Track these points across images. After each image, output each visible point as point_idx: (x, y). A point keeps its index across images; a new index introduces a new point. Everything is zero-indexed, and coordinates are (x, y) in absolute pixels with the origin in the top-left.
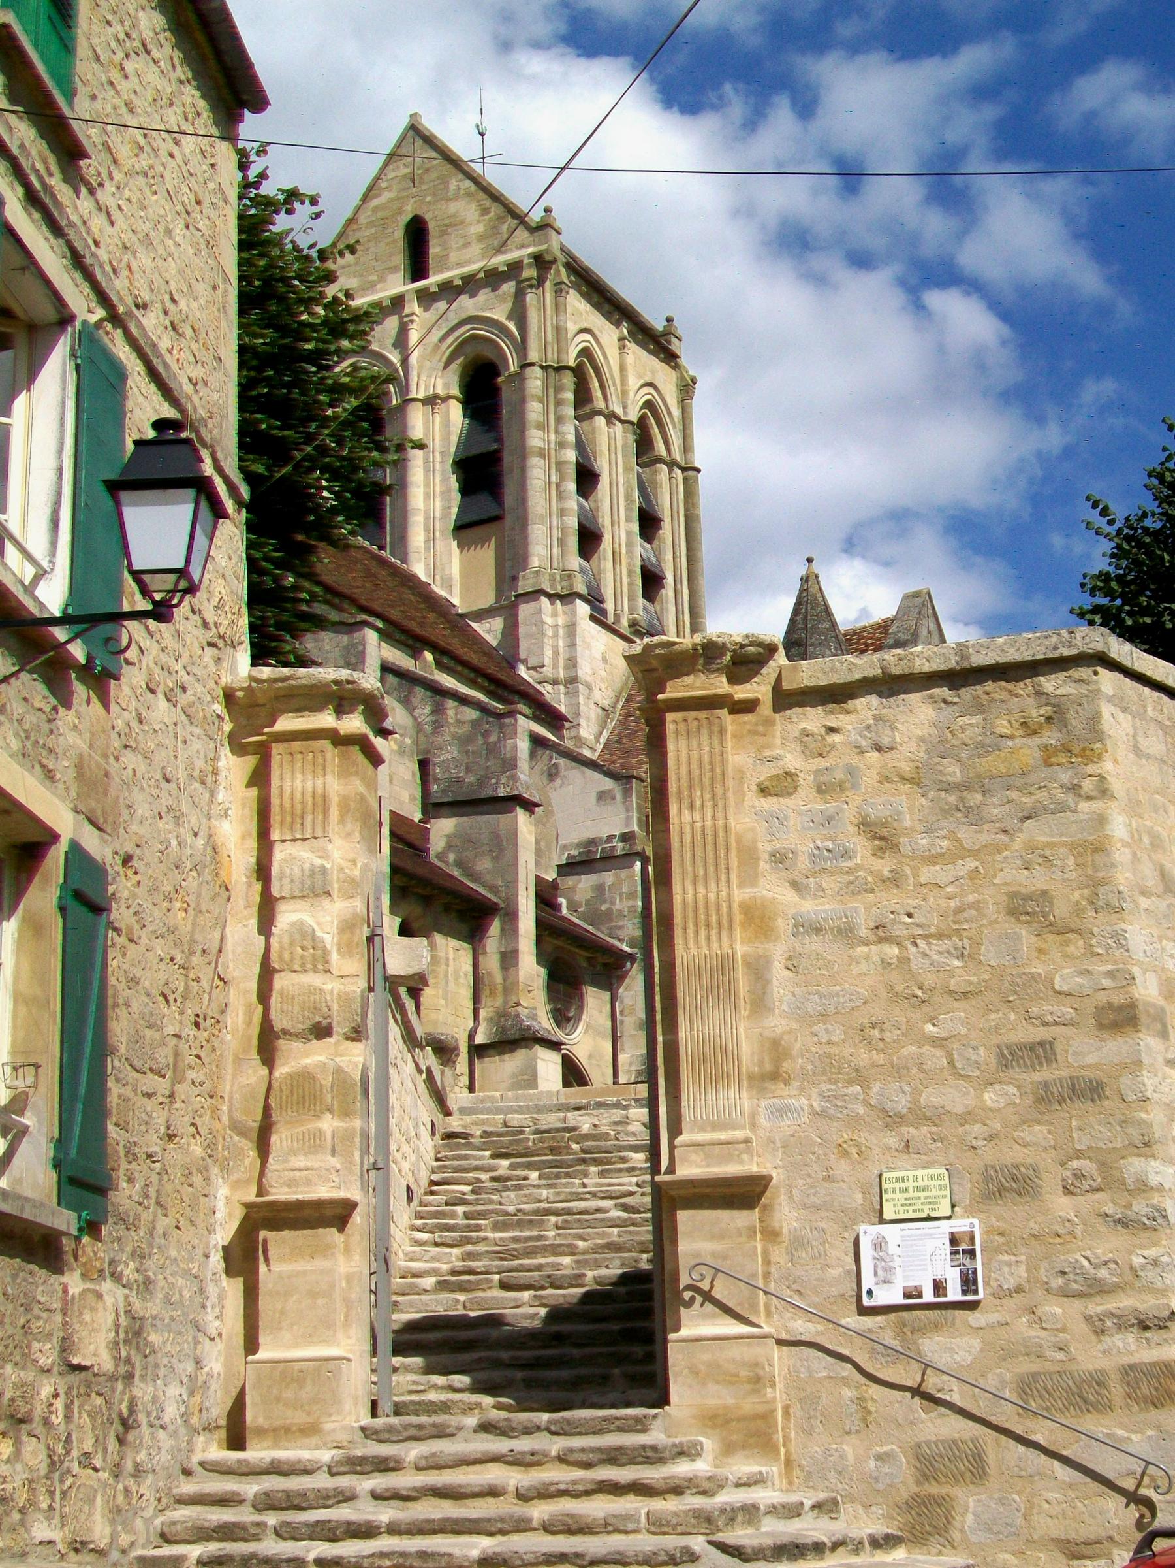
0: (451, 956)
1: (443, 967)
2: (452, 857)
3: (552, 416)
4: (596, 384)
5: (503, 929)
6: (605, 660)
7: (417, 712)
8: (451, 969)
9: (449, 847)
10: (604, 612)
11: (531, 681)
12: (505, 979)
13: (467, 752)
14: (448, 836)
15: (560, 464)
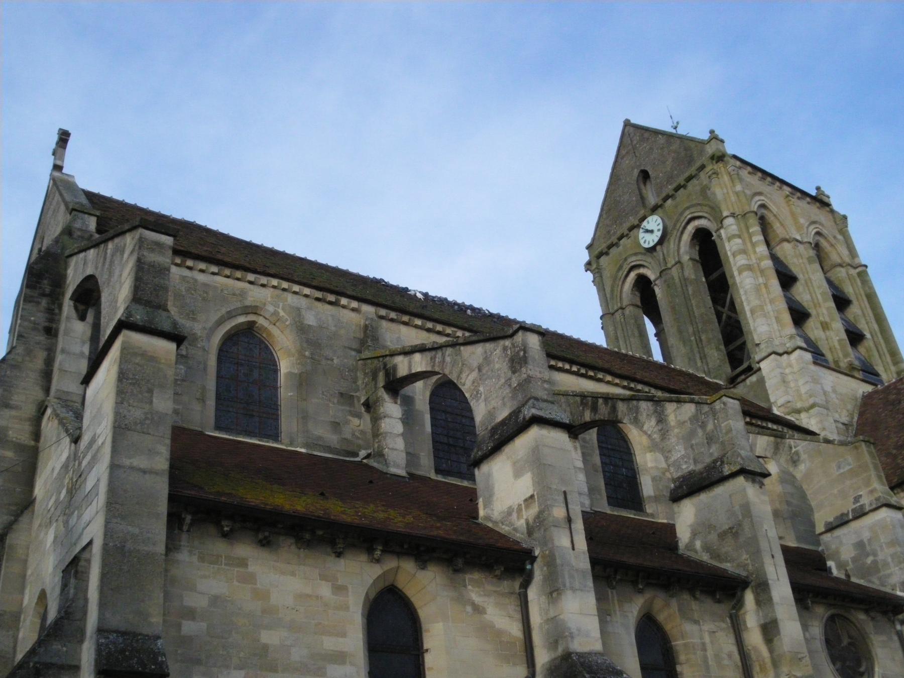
0: (707, 639)
1: (699, 653)
2: (698, 544)
3: (749, 245)
4: (778, 225)
5: (758, 603)
6: (834, 391)
7: (645, 428)
8: (710, 653)
9: (694, 534)
10: (826, 361)
11: (782, 415)
12: (771, 651)
13: (692, 446)
14: (691, 526)
15: (762, 272)
